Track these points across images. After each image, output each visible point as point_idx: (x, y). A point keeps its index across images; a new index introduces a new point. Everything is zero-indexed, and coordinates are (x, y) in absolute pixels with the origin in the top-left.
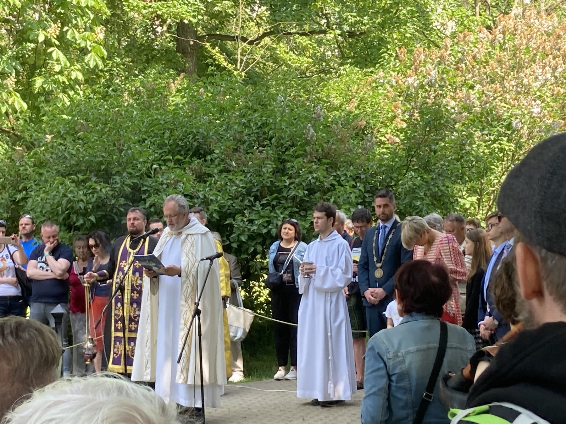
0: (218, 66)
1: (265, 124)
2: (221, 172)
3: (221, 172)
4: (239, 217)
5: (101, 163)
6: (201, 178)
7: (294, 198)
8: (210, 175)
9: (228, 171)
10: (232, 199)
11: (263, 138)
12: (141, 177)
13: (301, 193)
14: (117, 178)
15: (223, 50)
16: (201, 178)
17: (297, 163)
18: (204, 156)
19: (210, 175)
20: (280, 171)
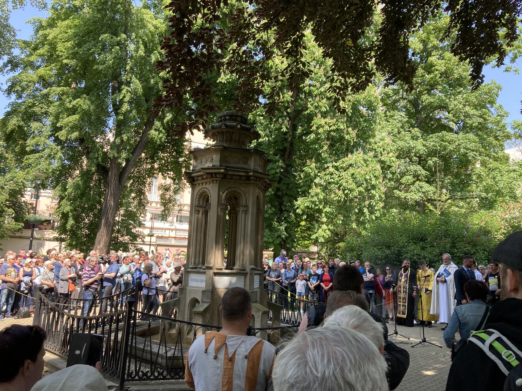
0: (430, 210)
1: (447, 230)
2: (430, 246)
3: (430, 246)
4: (437, 263)
5: (387, 243)
6: (423, 248)
7: (459, 257)
8: (426, 248)
9: (433, 246)
10: (434, 256)
11: (446, 234)
12: (401, 248)
13: (461, 255)
14: (392, 248)
15: (432, 204)
16: (423, 248)
17: (460, 244)
18: (425, 241)
19: (426, 248)
20: (453, 246)
